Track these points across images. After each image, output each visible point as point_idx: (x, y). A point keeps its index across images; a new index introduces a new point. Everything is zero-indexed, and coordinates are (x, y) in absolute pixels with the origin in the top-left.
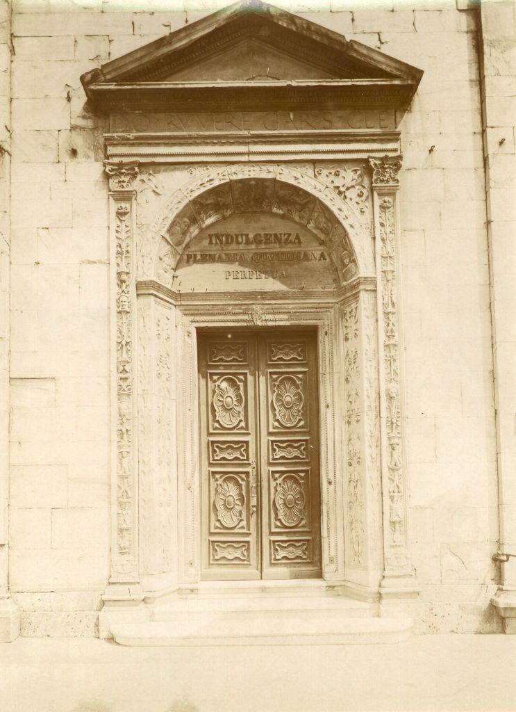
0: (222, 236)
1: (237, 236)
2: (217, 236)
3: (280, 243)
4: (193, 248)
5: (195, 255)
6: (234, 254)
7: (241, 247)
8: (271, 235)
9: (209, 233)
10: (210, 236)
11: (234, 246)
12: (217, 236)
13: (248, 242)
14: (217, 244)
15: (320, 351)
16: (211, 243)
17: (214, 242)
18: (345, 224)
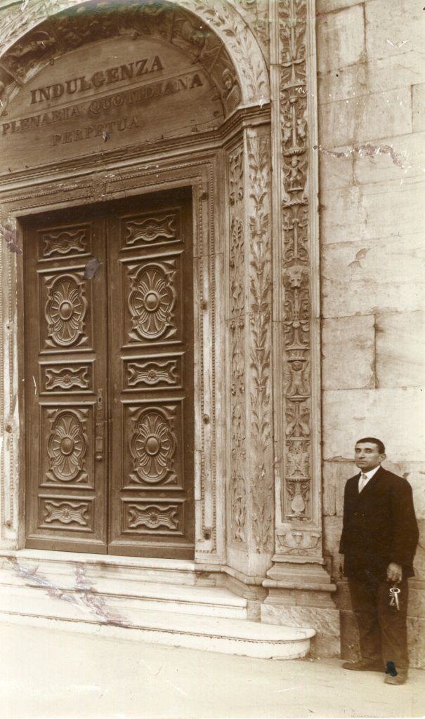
0: (49, 88)
1: (69, 83)
2: (42, 91)
3: (130, 77)
4: (10, 115)
5: (14, 123)
6: (64, 110)
7: (74, 97)
8: (116, 69)
9: (32, 89)
10: (33, 93)
11: (64, 98)
12: (42, 91)
13: (83, 90)
14: (41, 101)
15: (195, 224)
16: (34, 101)
17: (38, 99)
18: (219, 31)
